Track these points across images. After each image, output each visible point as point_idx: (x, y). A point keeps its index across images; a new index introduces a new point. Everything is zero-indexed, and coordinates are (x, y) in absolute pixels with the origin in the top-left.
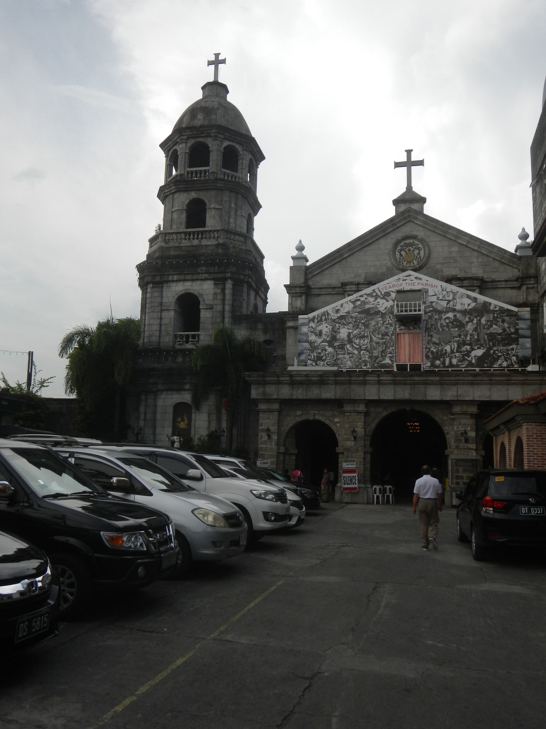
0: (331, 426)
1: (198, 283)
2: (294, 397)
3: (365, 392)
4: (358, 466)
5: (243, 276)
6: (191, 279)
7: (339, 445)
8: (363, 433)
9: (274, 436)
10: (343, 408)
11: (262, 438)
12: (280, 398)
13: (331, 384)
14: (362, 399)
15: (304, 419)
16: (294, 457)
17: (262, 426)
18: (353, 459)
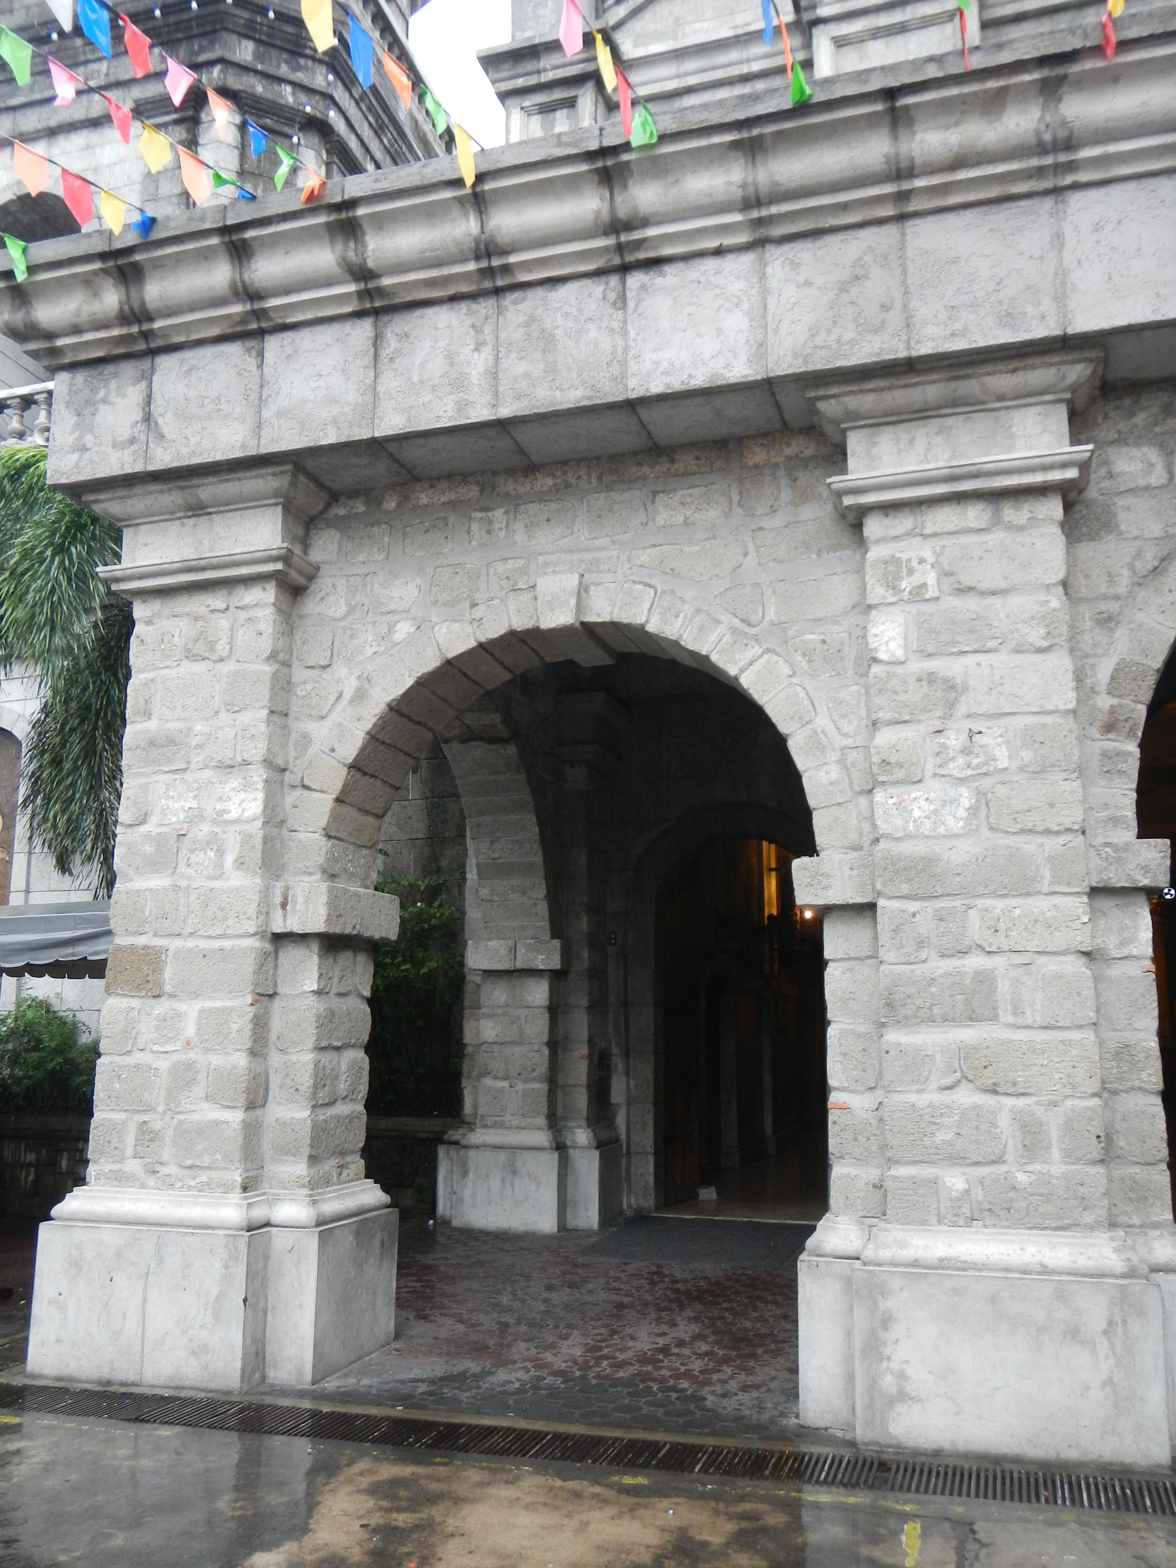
0: (732, 671)
1: (79, 139)
2: (391, 423)
3: (1062, 273)
4: (1041, 1036)
5: (294, 94)
6: (40, 126)
7: (819, 839)
8: (1066, 698)
9: (246, 787)
10: (846, 473)
11: (143, 821)
12: (276, 448)
13: (718, 252)
14: (1039, 332)
15: (494, 630)
16: (539, 993)
17: (148, 715)
18: (974, 962)
